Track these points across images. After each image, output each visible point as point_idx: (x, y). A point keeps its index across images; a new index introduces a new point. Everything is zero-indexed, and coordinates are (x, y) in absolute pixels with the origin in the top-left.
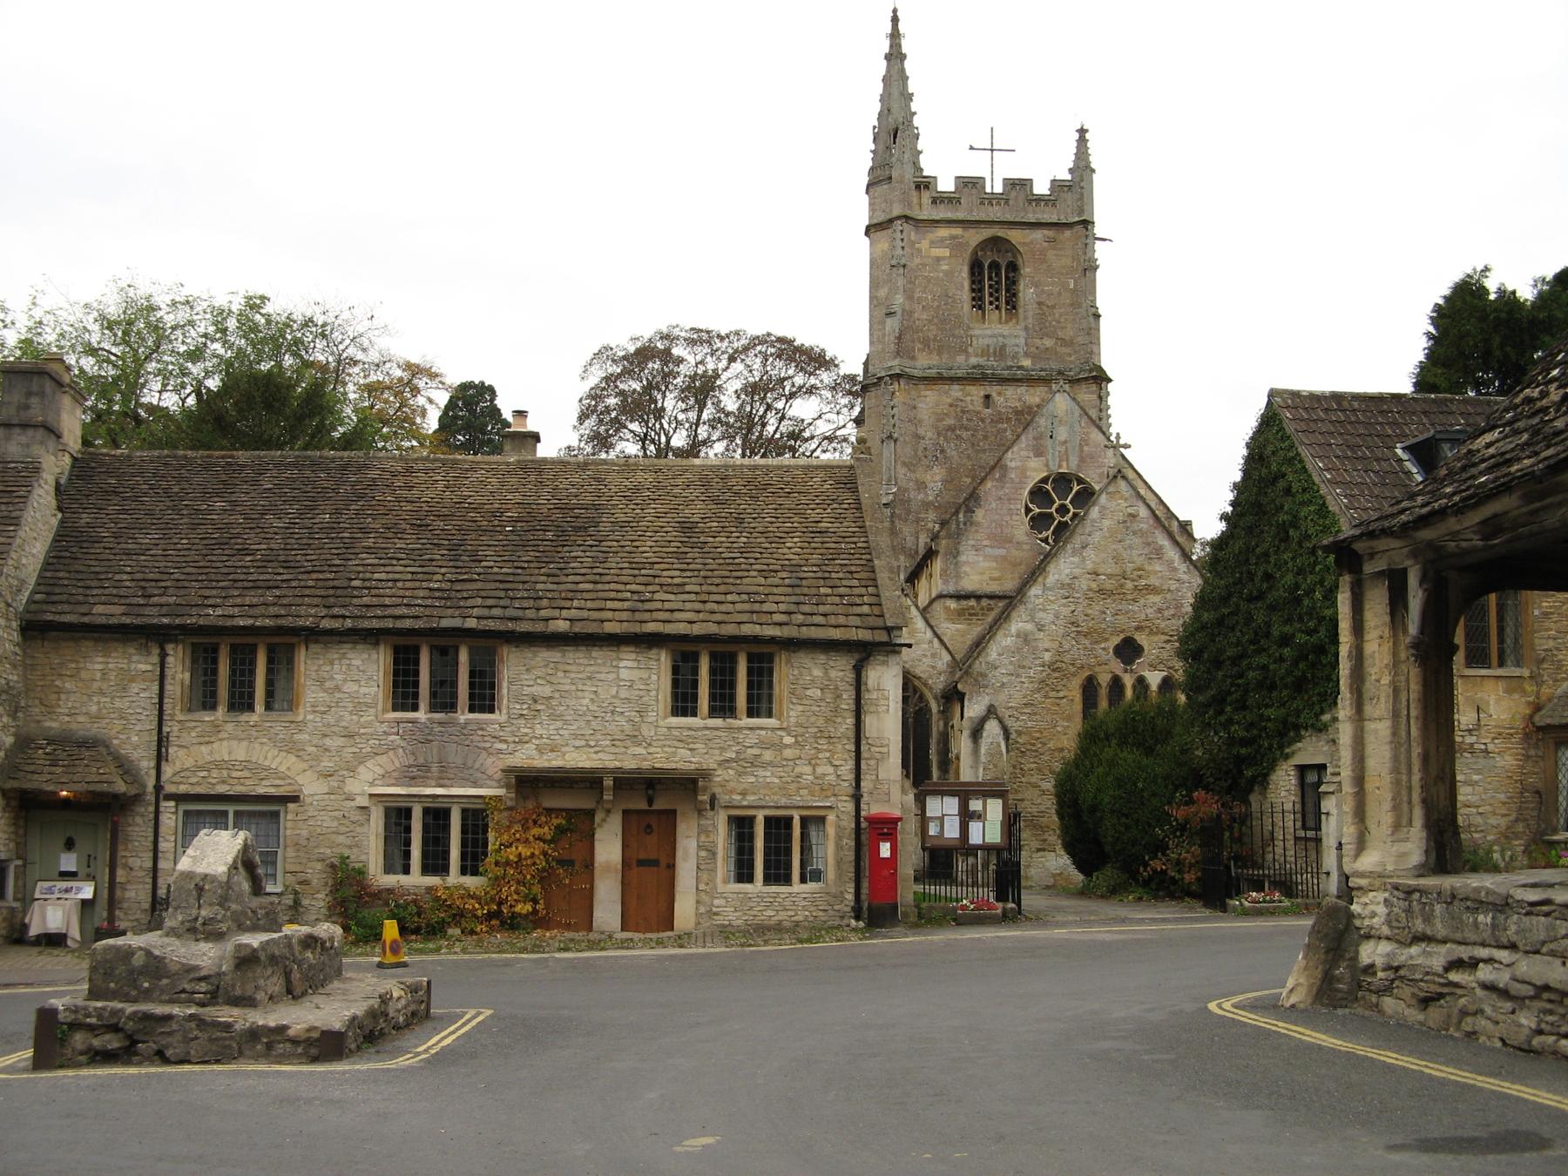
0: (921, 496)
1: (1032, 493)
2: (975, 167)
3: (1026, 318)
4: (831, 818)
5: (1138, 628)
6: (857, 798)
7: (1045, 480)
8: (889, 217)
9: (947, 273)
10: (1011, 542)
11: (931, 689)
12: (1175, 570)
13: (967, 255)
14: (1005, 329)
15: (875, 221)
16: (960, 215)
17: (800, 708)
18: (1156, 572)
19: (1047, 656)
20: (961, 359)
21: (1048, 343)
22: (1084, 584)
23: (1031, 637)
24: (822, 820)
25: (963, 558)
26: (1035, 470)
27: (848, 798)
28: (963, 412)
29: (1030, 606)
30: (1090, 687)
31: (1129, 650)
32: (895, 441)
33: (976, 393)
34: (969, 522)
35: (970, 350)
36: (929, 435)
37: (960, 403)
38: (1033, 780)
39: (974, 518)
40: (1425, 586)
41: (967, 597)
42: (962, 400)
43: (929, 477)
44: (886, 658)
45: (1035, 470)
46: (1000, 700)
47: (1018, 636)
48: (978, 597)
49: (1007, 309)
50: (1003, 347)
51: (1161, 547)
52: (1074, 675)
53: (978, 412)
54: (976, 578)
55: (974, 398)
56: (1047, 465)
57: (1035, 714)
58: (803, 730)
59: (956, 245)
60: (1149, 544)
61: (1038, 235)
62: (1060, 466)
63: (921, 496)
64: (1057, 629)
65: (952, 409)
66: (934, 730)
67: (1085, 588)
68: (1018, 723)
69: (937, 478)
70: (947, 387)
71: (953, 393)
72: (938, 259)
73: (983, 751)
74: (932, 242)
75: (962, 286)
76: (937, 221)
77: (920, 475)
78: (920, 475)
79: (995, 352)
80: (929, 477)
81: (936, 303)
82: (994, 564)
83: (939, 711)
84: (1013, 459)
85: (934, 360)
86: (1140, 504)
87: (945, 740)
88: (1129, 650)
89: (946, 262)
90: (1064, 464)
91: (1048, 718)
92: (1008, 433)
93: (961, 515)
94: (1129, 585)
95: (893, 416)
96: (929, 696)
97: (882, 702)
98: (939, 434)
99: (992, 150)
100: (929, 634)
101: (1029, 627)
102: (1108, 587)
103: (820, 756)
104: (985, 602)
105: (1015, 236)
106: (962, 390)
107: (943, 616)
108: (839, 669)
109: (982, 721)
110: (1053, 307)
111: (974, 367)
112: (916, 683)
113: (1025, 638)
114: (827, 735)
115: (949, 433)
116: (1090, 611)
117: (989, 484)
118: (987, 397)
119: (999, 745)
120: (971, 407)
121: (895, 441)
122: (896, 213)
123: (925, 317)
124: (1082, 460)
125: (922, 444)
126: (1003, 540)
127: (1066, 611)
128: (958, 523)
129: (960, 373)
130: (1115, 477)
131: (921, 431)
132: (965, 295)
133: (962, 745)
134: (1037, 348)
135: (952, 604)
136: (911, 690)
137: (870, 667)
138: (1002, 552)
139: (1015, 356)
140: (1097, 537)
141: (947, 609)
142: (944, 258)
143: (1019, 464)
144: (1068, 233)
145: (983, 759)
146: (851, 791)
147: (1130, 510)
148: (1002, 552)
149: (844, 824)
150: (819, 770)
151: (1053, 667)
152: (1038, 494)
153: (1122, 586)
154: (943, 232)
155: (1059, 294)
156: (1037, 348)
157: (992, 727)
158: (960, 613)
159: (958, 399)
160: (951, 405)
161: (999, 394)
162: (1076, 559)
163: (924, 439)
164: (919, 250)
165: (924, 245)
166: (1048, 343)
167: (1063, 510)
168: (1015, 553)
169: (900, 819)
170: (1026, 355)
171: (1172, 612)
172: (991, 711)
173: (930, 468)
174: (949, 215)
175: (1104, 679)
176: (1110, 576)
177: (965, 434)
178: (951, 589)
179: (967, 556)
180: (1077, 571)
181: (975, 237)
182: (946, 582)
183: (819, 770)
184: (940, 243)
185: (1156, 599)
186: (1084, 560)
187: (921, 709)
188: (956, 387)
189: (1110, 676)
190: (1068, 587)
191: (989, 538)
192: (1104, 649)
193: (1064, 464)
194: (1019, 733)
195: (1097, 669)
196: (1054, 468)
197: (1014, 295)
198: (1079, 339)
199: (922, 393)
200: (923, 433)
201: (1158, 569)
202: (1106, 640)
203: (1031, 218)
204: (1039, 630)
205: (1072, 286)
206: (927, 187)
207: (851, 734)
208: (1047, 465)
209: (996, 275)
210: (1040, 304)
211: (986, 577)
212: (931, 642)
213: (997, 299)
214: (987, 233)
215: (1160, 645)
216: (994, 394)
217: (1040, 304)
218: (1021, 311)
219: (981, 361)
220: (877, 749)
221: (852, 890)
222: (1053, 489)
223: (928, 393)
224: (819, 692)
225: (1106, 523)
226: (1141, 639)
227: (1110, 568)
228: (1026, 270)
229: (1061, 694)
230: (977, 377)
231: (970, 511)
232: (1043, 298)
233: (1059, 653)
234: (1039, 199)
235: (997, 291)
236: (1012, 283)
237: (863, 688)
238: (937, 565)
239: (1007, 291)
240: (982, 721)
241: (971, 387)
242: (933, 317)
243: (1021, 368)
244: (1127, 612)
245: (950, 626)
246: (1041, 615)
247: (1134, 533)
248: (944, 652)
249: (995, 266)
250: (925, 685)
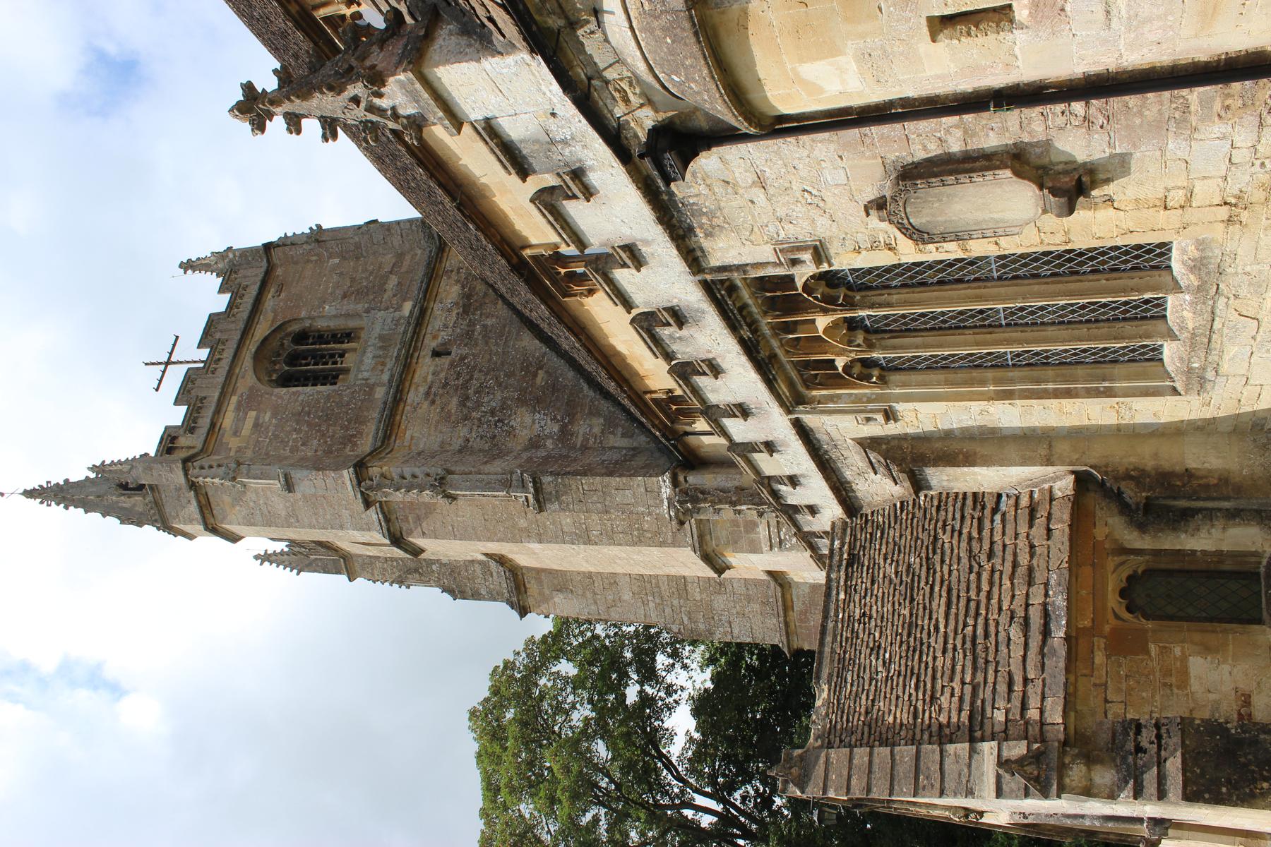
0: (549, 444)
2: (176, 376)
3: (357, 315)
9: (274, 415)
13: (264, 388)
15: (197, 516)
16: (216, 395)
28: (445, 385)
32: (449, 472)
33: (426, 368)
35: (371, 381)
37: (433, 390)
42: (430, 388)
43: (525, 432)
50: (381, 338)
53: (451, 364)
55: (431, 369)
61: (269, 302)
63: (549, 443)
65: (438, 401)
69: (528, 419)
70: (408, 408)
71: (417, 400)
72: (256, 425)
75: (294, 393)
77: (516, 445)
78: (516, 445)
80: (525, 432)
81: (305, 428)
92: (489, 322)
95: (414, 476)
98: (466, 418)
99: (168, 363)
105: (262, 329)
106: (416, 389)
110: (353, 280)
115: (469, 404)
118: (436, 354)
120: (442, 375)
121: (449, 472)
122: (182, 480)
123: (315, 442)
125: (477, 444)
131: (457, 443)
132: (307, 392)
134: (394, 296)
139: (397, 322)
142: (257, 418)
154: (228, 420)
155: (341, 274)
156: (394, 296)
159: (427, 394)
160: (433, 402)
163: (468, 440)
164: (239, 450)
165: (234, 443)
166: (393, 281)
170: (399, 308)
173: (511, 432)
181: (247, 378)
184: (239, 421)
198: (396, 243)
199: (406, 444)
200: (460, 441)
205: (337, 261)
206: (173, 439)
209: (305, 358)
210: (344, 296)
213: (332, 356)
216: (434, 344)
217: (344, 296)
219: (390, 364)
223: (408, 433)
230: (407, 366)
232: (339, 292)
234: (231, 305)
235: (323, 356)
236: (321, 337)
241: (416, 376)
242: (319, 431)
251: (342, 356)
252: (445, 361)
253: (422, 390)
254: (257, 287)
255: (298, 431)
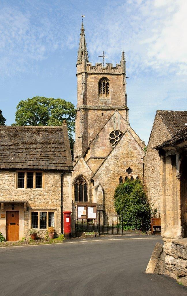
1: (110, 135)
4: (55, 212)
5: (131, 165)
6: (62, 208)
7: (113, 132)
8: (81, 72)
10: (106, 146)
11: (87, 179)
12: (139, 152)
14: (106, 98)
16: (97, 72)
17: (48, 186)
18: (135, 153)
19: (112, 172)
20: (97, 105)
21: (116, 101)
22: (120, 155)
23: (108, 167)
24: (53, 213)
25: (95, 149)
26: (111, 129)
27: (59, 207)
28: (97, 116)
29: (108, 160)
30: (121, 179)
31: (129, 170)
33: (100, 112)
34: (97, 141)
35: (99, 103)
36: (90, 121)
37: (97, 115)
38: (109, 200)
39: (98, 140)
40: (181, 160)
41: (96, 158)
44: (68, 174)
45: (111, 129)
46: (102, 182)
47: (105, 167)
48: (99, 158)
49: (107, 94)
51: (137, 147)
52: (117, 176)
54: (98, 154)
56: (114, 129)
57: (109, 185)
58: (49, 191)
59: (96, 79)
60: (134, 146)
61: (114, 76)
62: (116, 129)
64: (114, 166)
66: (88, 188)
67: (120, 156)
68: (106, 187)
69: (92, 131)
72: (92, 82)
73: (98, 193)
74: (91, 78)
76: (92, 73)
79: (104, 103)
82: (102, 151)
83: (89, 184)
84: (106, 127)
85: (91, 105)
86: (132, 137)
87: (91, 190)
88: (129, 170)
89: (94, 82)
90: (117, 128)
91: (112, 186)
93: (95, 140)
94: (130, 156)
96: (87, 181)
97: (67, 184)
99: (104, 57)
100: (87, 166)
101: (108, 165)
102: (125, 156)
103: (53, 197)
104: (100, 159)
107: (91, 162)
108: (58, 177)
109: (98, 186)
111: (100, 106)
112: (85, 178)
113: (107, 168)
114: (54, 192)
116: (121, 162)
117: (101, 133)
118: (102, 113)
119: (101, 192)
120: (99, 115)
124: (121, 127)
126: (104, 145)
127: (116, 162)
128: (94, 142)
129: (97, 108)
130: (126, 131)
132: (97, 90)
133: (94, 192)
135: (93, 160)
136: (83, 179)
137: (64, 176)
138: (104, 148)
139: (109, 104)
140: (122, 145)
141: (92, 161)
142: (93, 82)
143: (107, 128)
144: (120, 76)
145: (98, 195)
146: (60, 206)
147: (130, 139)
148: (104, 148)
149: (59, 213)
150: (53, 201)
151: (113, 174)
152: (111, 135)
153: (128, 156)
154: (93, 76)
157: (100, 188)
158: (95, 162)
160: (95, 115)
161: (105, 112)
162: (118, 150)
166: (116, 101)
167: (117, 138)
168: (107, 148)
169: (71, 213)
170: (111, 104)
171: (139, 162)
172: (100, 185)
174: (95, 72)
175: (124, 177)
176: (125, 154)
177: (98, 122)
178: (93, 156)
179: (96, 149)
180: (118, 153)
181: (100, 77)
182: (92, 155)
183: (53, 201)
185: (135, 159)
186: (120, 150)
187: (85, 184)
188: (96, 111)
189: (126, 176)
190: (116, 156)
191: (101, 145)
192: (124, 170)
193: (117, 128)
194: (106, 189)
195: (123, 175)
196: (115, 129)
197: (108, 90)
201: (136, 152)
202: (125, 168)
203: (112, 73)
204: (110, 166)
207: (60, 192)
208: (114, 129)
210: (114, 92)
211: (100, 154)
212: (87, 168)
213: (105, 91)
214: (103, 76)
215: (137, 169)
216: (104, 113)
217: (114, 92)
218: (110, 94)
219: (101, 105)
220: (66, 196)
221: (61, 230)
222: (115, 134)
224: (52, 182)
225: (124, 142)
226: (132, 168)
227: (125, 152)
228: (110, 85)
229: (115, 180)
231: (97, 139)
233: (114, 171)
235: (105, 89)
236: (108, 88)
237: (63, 181)
238: (89, 152)
239: (107, 89)
240: (98, 186)
243: (110, 107)
244: (129, 162)
245: (93, 164)
246: (110, 162)
247: (131, 144)
248: (90, 171)
249: (104, 84)
250: (86, 178)
251: (105, 93)
252: (101, 115)
253: (97, 113)
254: (117, 73)
255: (91, 91)
